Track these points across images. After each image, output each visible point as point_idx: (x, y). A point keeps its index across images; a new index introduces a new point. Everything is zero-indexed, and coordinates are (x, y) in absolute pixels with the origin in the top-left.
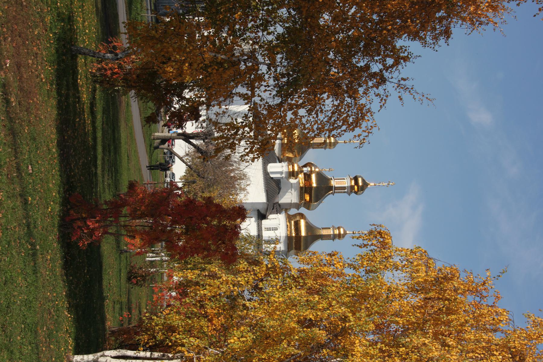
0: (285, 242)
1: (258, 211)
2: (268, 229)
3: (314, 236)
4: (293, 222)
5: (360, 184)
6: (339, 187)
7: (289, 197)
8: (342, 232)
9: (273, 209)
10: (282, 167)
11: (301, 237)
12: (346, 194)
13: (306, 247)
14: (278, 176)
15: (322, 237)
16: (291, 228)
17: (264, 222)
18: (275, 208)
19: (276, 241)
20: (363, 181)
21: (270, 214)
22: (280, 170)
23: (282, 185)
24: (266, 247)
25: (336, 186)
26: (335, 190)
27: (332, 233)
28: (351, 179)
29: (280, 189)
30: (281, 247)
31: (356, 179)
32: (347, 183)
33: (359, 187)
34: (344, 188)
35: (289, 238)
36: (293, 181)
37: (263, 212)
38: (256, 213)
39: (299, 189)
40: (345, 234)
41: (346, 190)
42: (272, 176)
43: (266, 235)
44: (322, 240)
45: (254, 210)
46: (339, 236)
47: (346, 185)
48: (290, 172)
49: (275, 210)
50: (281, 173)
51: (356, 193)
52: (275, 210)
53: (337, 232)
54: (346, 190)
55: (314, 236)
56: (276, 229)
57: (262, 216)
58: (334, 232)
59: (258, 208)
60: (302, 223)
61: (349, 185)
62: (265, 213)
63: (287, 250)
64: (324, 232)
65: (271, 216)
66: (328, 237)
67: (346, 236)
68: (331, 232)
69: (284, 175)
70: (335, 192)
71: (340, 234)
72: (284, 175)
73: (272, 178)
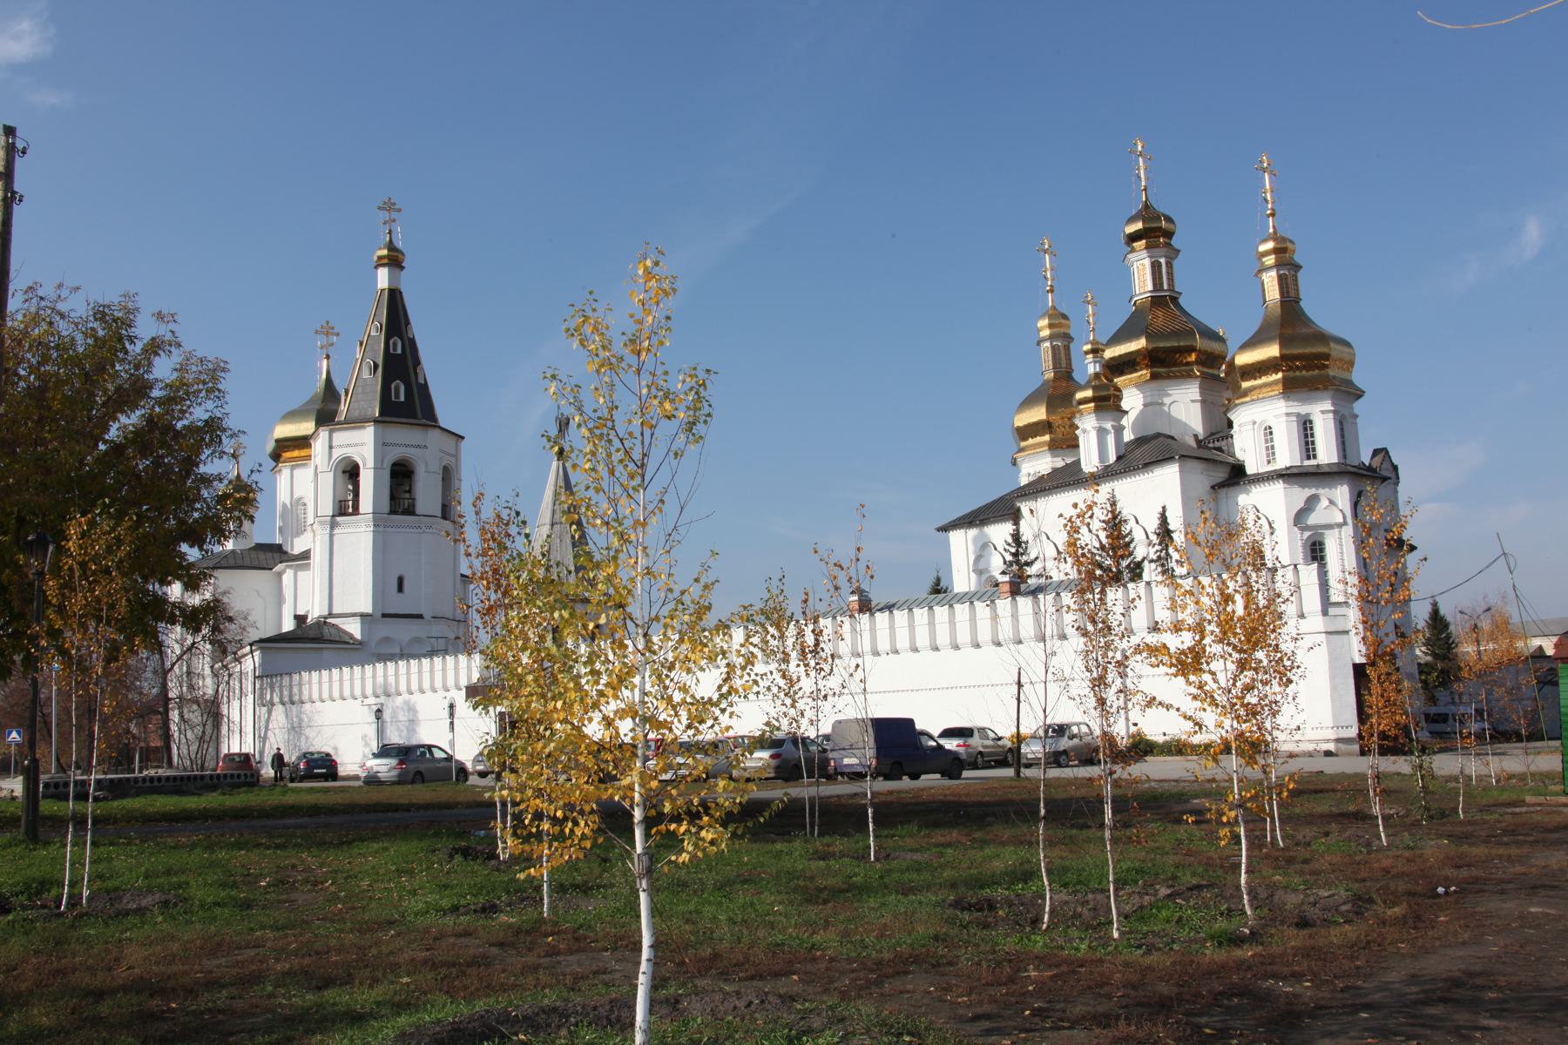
0: (1304, 401)
1: (1215, 487)
2: (1271, 452)
3: (1289, 320)
4: (1245, 385)
5: (1139, 226)
6: (1154, 279)
7: (1185, 406)
8: (1270, 245)
9: (1220, 449)
10: (1084, 431)
11: (1283, 357)
12: (1176, 263)
13: (1322, 337)
14: (1111, 440)
15: (1290, 300)
16: (1261, 387)
17: (1250, 470)
18: (1217, 444)
19: (1306, 426)
20: (1131, 220)
21: (1233, 455)
22: (1093, 436)
23: (1151, 432)
24: (1326, 453)
25: (1150, 287)
26: (1162, 289)
27: (1273, 273)
28: (1133, 250)
29: (1158, 435)
30: (1321, 413)
31: (1134, 238)
32: (1140, 266)
33: (1155, 232)
34: (1156, 267)
35: (1291, 388)
36: (1133, 400)
37: (1221, 475)
38: (1223, 492)
39: (1155, 384)
40: (1275, 237)
41: (1162, 261)
42: (1112, 458)
43: (1288, 455)
44: (1297, 300)
45: (1216, 500)
46: (1282, 251)
47: (1147, 262)
48: (1097, 410)
49: (1223, 444)
50: (1101, 432)
51: (1169, 235)
52: (1223, 444)
53: (1270, 260)
54: (1162, 261)
55: (1289, 320)
56: (1269, 431)
57: (1237, 475)
58: (1270, 268)
59: (1208, 487)
60: (1243, 359)
61: (1144, 254)
62: (1228, 469)
63: (1329, 393)
64: (1273, 293)
65: (1239, 455)
66: (1287, 285)
67: (1281, 233)
68: (1270, 280)
69: (1108, 425)
70: (1171, 289)
71: (1276, 251)
72: (1108, 425)
73: (1119, 458)
